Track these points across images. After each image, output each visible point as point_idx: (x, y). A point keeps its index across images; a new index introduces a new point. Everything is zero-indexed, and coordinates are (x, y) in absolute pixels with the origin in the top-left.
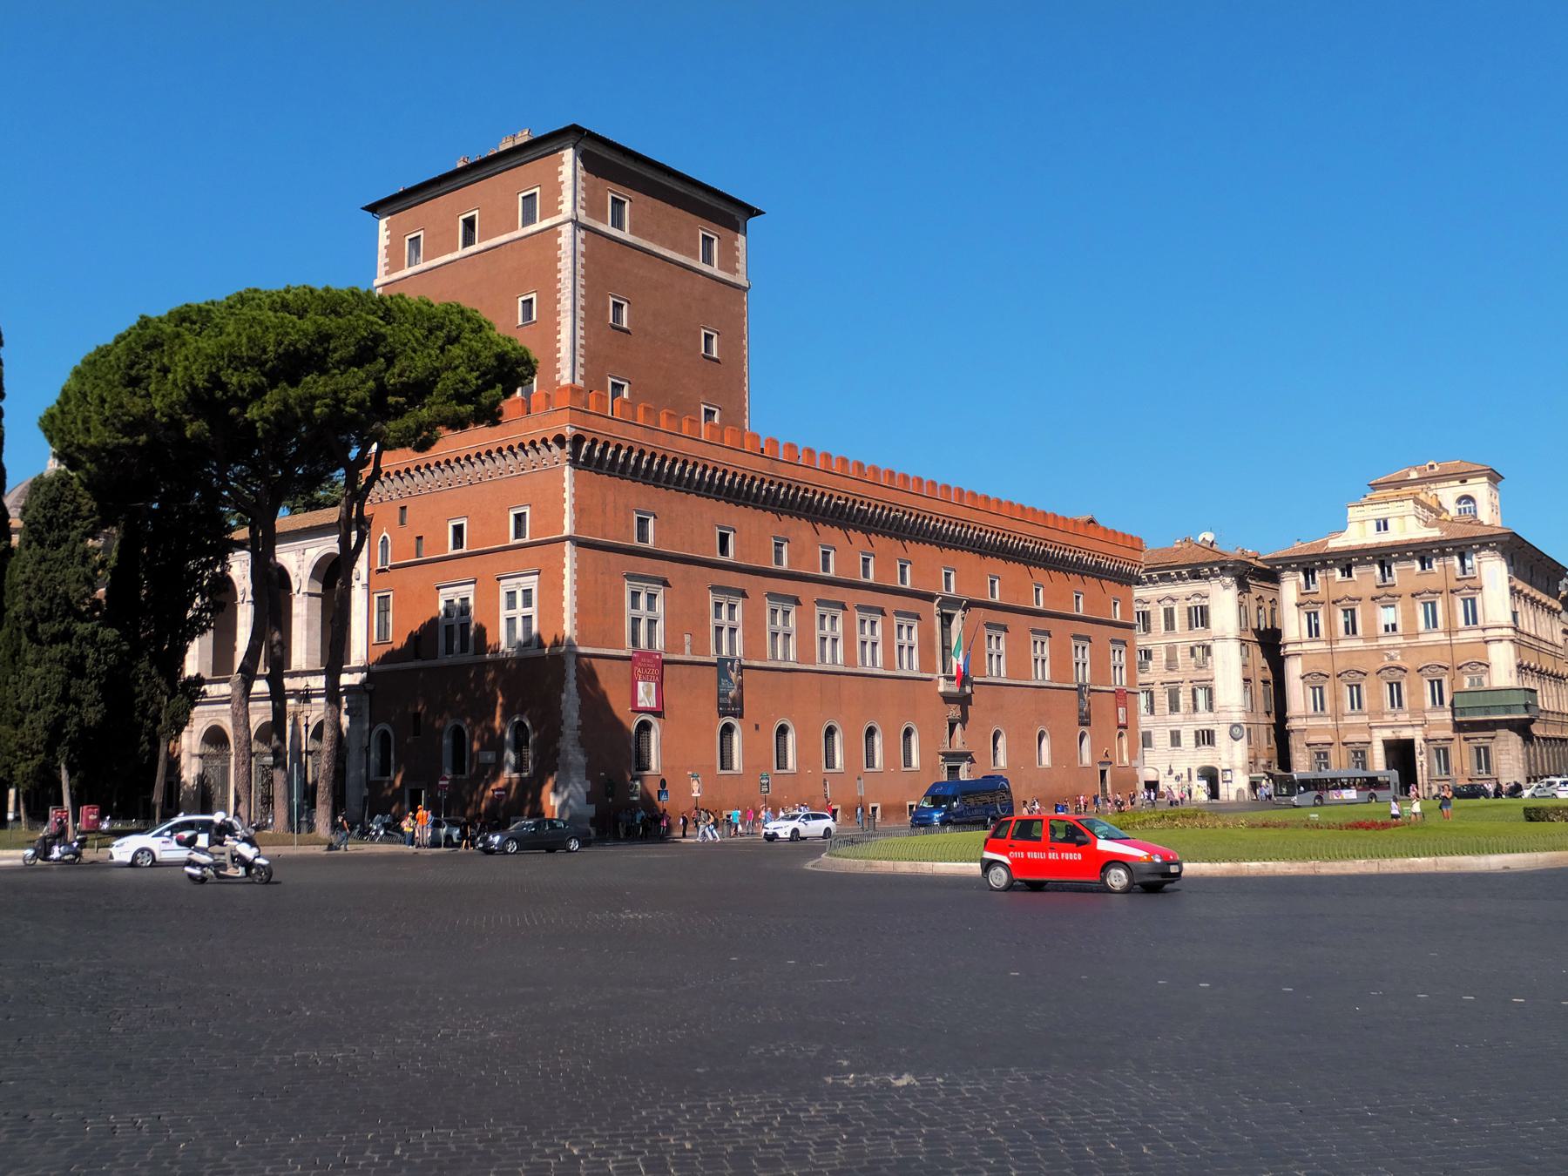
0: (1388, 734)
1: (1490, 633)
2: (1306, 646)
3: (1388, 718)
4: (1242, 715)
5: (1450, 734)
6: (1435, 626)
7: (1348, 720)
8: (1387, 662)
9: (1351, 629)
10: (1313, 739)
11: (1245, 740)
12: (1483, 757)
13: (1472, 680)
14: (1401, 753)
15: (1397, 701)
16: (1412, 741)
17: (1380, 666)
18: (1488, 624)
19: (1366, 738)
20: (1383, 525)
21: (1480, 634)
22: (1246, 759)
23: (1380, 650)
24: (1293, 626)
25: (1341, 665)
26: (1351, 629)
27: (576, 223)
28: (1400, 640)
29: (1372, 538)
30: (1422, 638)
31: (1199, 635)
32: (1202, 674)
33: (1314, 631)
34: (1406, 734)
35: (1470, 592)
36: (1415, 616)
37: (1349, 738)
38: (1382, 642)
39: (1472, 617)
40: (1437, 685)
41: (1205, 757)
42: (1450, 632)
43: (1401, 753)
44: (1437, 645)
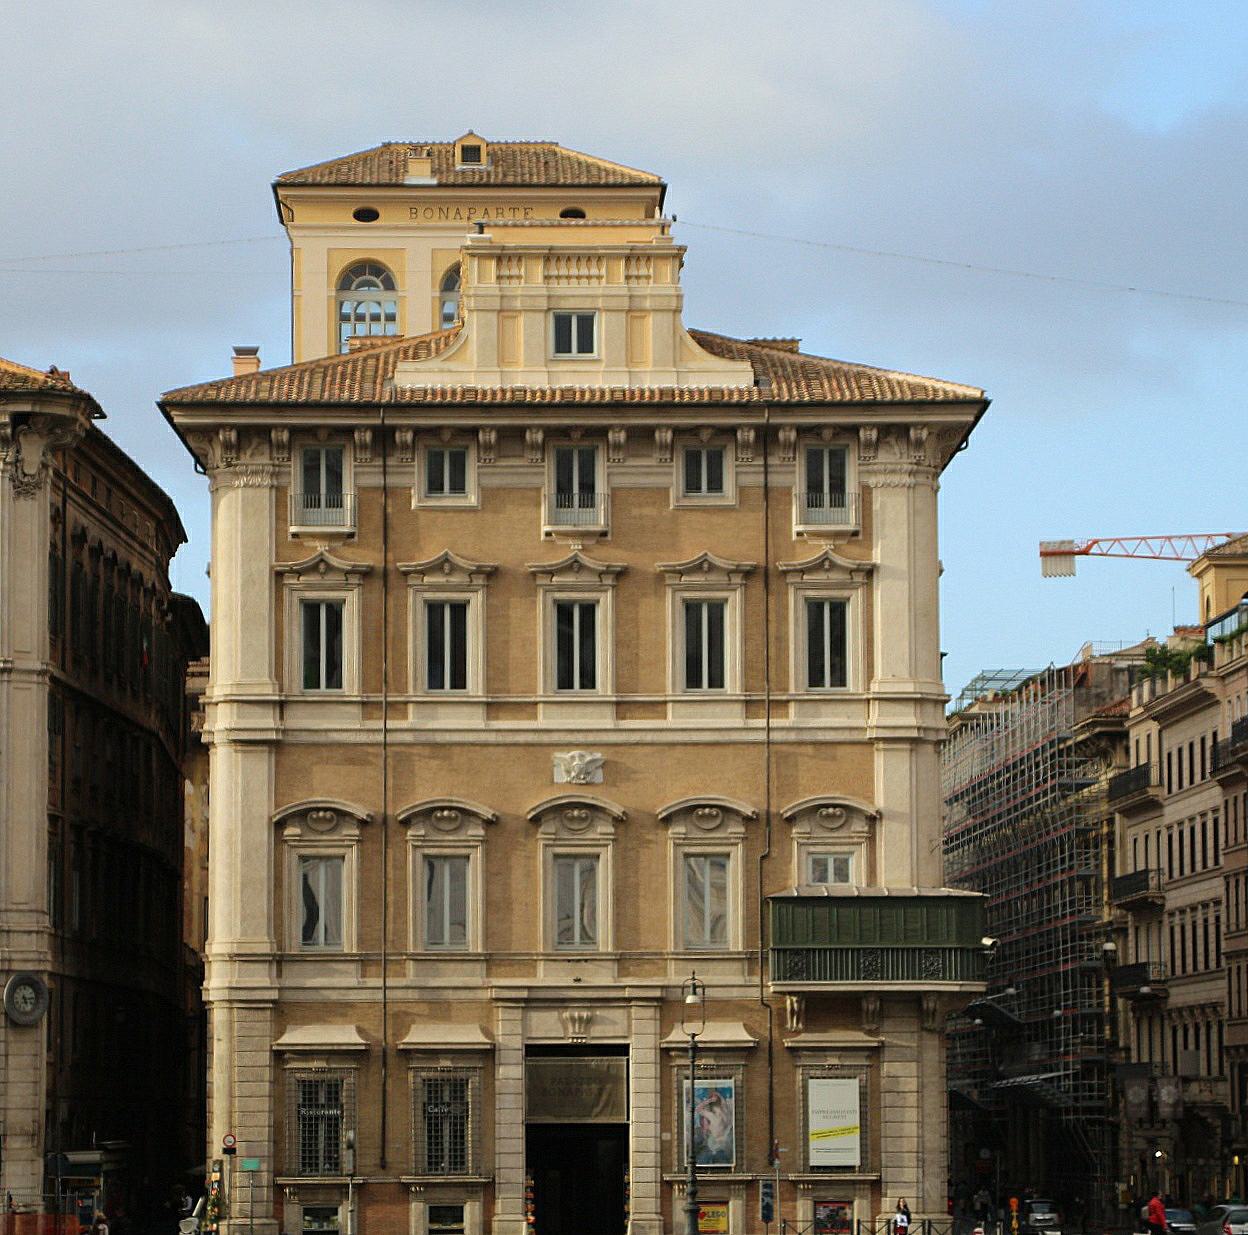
0: (550, 1027)
2: (298, 719)
10: (297, 1036)
19: (469, 1035)
20: (572, 333)
26: (446, 665)
28: (606, 720)
33: (321, 664)
34: (608, 1028)
39: (827, 660)
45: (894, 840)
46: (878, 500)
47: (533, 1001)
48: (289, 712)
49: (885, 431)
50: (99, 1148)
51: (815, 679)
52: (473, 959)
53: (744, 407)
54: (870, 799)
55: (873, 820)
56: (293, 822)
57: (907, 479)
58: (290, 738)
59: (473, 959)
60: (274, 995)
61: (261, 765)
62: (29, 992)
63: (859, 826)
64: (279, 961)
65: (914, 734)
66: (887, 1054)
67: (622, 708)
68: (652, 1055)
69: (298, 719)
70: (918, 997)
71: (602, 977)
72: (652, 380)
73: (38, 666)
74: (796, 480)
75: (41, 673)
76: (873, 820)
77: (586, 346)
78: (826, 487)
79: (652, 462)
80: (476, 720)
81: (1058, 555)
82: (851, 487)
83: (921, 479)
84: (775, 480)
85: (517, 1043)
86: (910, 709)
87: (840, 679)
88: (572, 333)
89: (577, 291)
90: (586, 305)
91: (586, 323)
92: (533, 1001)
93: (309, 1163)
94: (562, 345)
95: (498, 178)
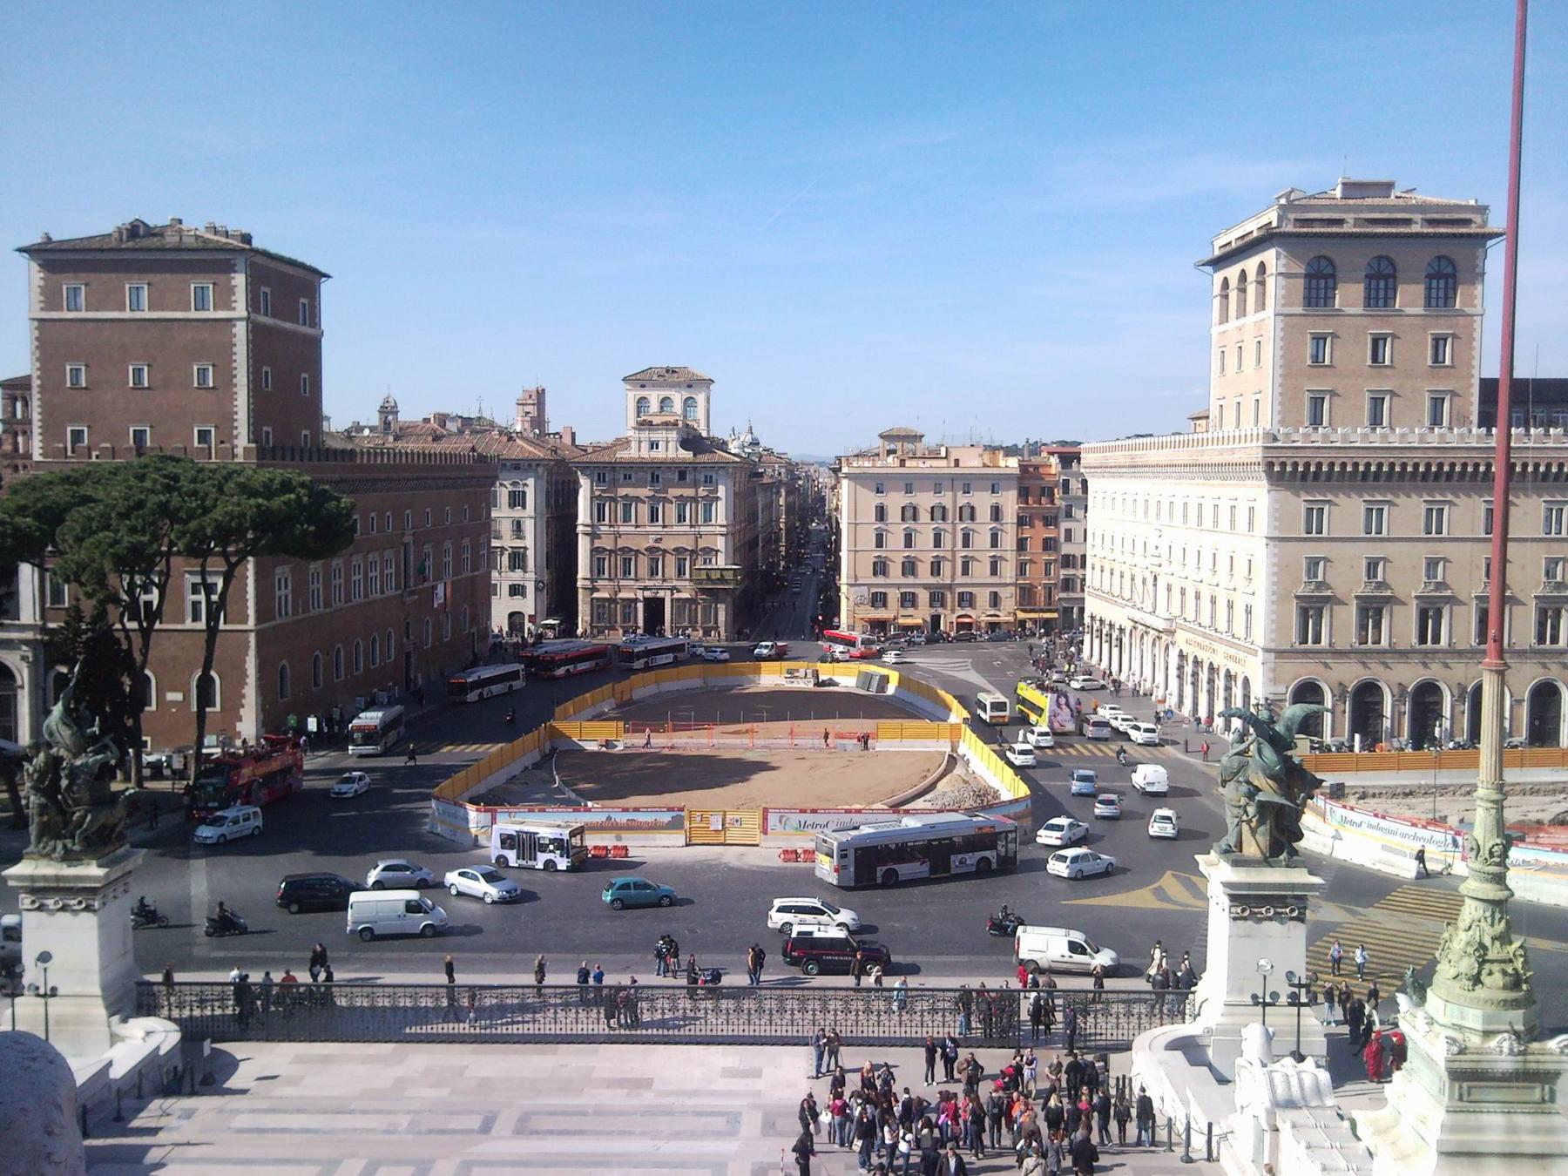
0: (648, 594)
3: (648, 583)
8: (651, 543)
10: (596, 595)
14: (654, 608)
15: (653, 572)
19: (632, 596)
20: (654, 445)
23: (647, 534)
24: (583, 514)
25: (621, 543)
26: (626, 519)
27: (248, 319)
29: (645, 453)
31: (517, 512)
32: (518, 543)
34: (661, 594)
35: (711, 499)
39: (707, 519)
41: (517, 604)
43: (654, 608)
44: (685, 534)
45: (721, 557)
47: (645, 588)
56: (594, 551)
61: (588, 539)
64: (592, 580)
72: (671, 454)
88: (654, 445)
89: (655, 436)
92: (645, 588)
95: (669, 376)
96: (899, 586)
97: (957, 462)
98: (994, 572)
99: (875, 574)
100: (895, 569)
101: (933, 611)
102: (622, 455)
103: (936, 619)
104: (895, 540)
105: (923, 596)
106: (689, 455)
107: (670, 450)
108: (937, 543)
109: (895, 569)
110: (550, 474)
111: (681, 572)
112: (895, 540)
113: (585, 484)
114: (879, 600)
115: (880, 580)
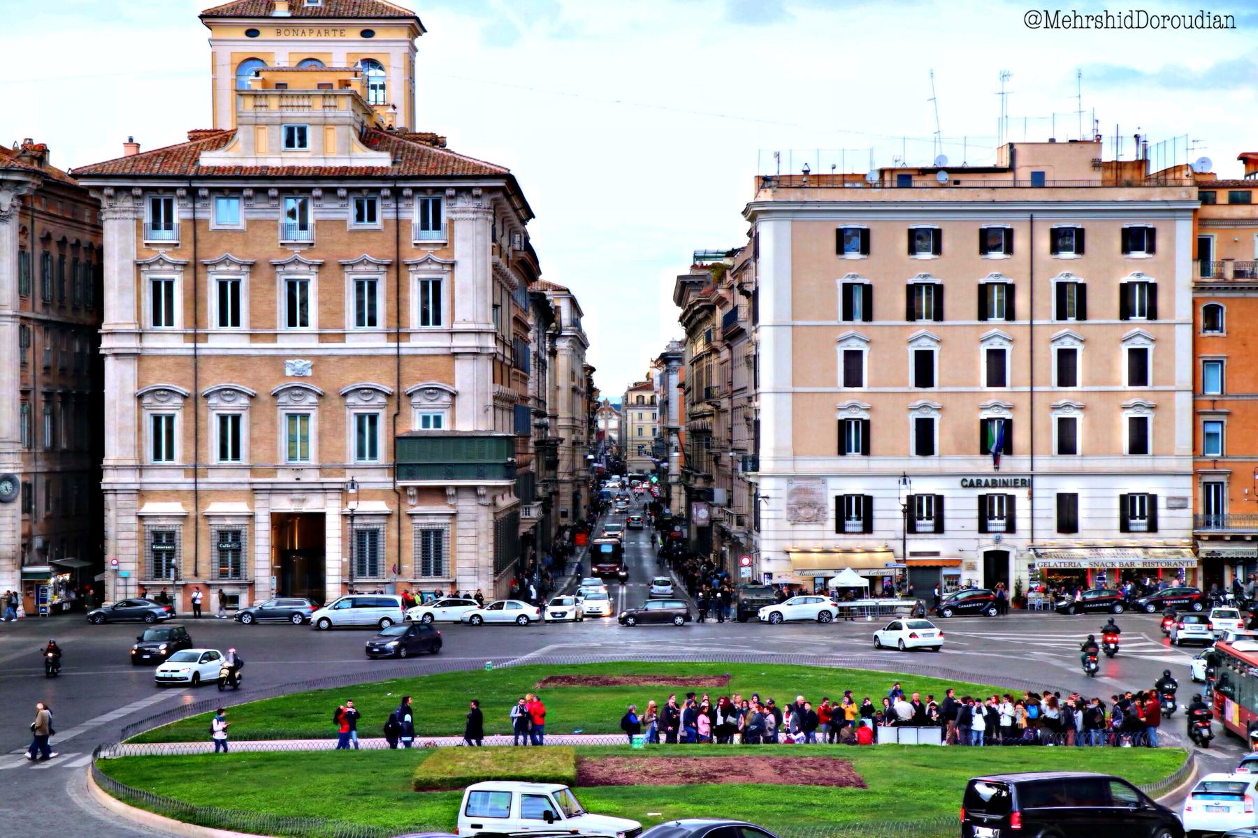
0: (285, 505)
1: (461, 343)
2: (150, 343)
3: (284, 477)
4: (17, 459)
5: (381, 506)
6: (372, 322)
7: (214, 477)
9: (230, 314)
10: (150, 508)
11: (17, 505)
12: (433, 547)
13: (426, 420)
16: (318, 520)
17: (276, 388)
18: (457, 327)
19: (242, 507)
21: (444, 341)
22: (18, 540)
26: (230, 314)
28: (314, 343)
30: (351, 342)
34: (312, 505)
36: (341, 304)
37: (215, 507)
38: (282, 343)
40: (368, 422)
42: (398, 335)
46: (458, 227)
48: (145, 338)
49: (459, 190)
50: (50, 564)
51: (425, 321)
52: (245, 468)
53: (384, 178)
54: (452, 384)
55: (453, 395)
57: (472, 216)
58: (145, 352)
59: (245, 468)
60: (137, 487)
62: (8, 485)
63: (446, 398)
65: (475, 350)
66: (460, 518)
67: (322, 337)
68: (339, 519)
69: (150, 343)
70: (475, 488)
71: (312, 477)
73: (11, 313)
74: (413, 214)
75: (13, 316)
76: (453, 395)
77: (303, 144)
78: (432, 220)
79: (336, 206)
80: (245, 343)
81: (778, 155)
82: (444, 220)
83: (480, 215)
84: (403, 216)
85: (267, 512)
86: (473, 336)
87: (437, 321)
88: (295, 137)
89: (296, 116)
90: (302, 122)
91: (303, 132)
92: (273, 491)
93: (158, 574)
94: (290, 143)
96: (905, 477)
97: (1038, 180)
98: (1139, 445)
99: (843, 450)
100: (895, 434)
101: (988, 543)
102: (209, 159)
103: (997, 563)
104: (888, 367)
105: (961, 508)
106: (380, 160)
107: (335, 149)
108: (997, 376)
109: (895, 434)
110: (25, 211)
111: (367, 448)
112: (888, 367)
113: (120, 238)
114: (855, 512)
115: (854, 461)
